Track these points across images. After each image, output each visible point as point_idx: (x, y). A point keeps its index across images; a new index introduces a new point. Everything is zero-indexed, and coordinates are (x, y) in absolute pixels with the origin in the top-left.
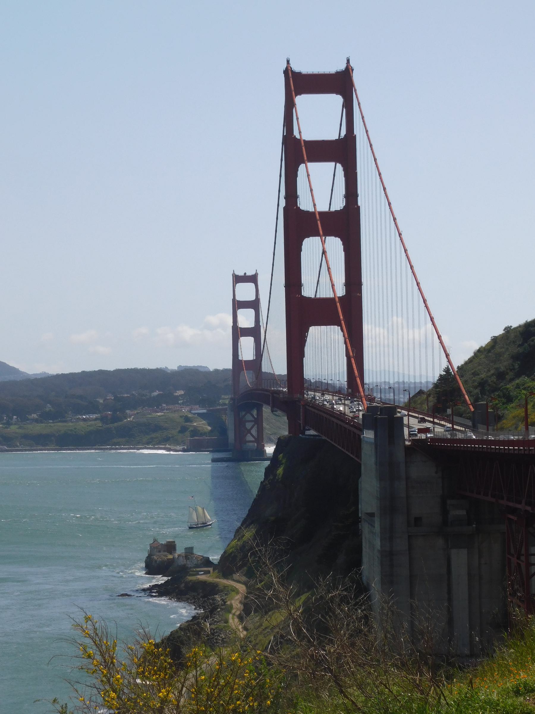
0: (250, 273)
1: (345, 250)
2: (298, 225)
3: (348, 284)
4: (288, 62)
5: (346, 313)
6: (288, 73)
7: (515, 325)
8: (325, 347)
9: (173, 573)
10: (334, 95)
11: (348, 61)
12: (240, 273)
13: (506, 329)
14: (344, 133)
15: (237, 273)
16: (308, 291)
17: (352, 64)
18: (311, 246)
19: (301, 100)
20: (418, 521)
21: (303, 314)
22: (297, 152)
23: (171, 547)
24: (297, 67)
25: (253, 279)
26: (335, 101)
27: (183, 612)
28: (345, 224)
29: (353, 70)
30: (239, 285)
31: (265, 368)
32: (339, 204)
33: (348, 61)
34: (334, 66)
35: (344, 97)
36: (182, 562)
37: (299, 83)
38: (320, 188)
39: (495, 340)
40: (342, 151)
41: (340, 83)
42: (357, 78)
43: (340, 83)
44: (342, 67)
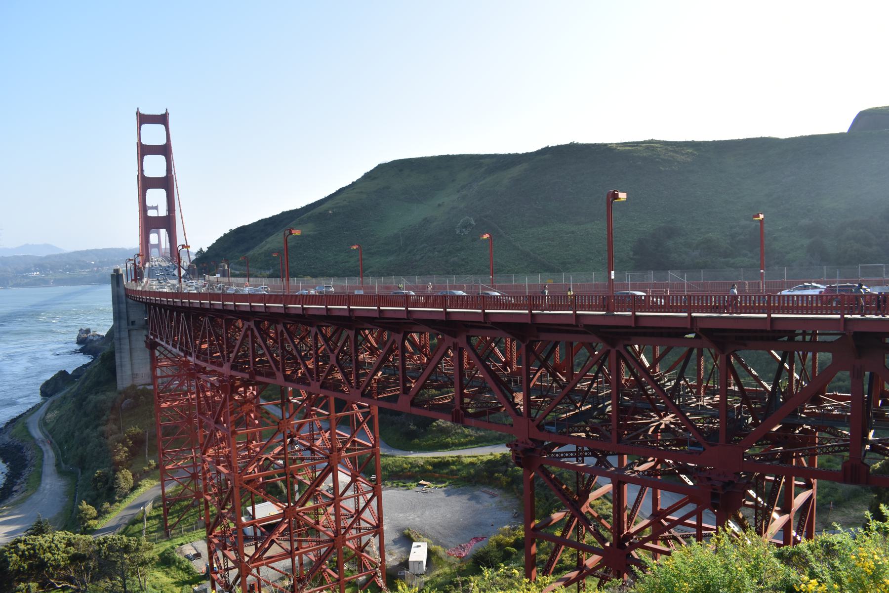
2: (146, 183)
5: (168, 223)
6: (138, 114)
7: (234, 228)
8: (158, 238)
9: (86, 343)
16: (151, 213)
19: (144, 126)
20: (133, 323)
22: (144, 150)
23: (88, 331)
24: (142, 112)
25: (156, 208)
28: (166, 183)
31: (163, 246)
34: (160, 112)
36: (91, 338)
37: (143, 119)
38: (155, 166)
39: (225, 235)
40: (165, 150)
43: (162, 119)
44: (164, 112)
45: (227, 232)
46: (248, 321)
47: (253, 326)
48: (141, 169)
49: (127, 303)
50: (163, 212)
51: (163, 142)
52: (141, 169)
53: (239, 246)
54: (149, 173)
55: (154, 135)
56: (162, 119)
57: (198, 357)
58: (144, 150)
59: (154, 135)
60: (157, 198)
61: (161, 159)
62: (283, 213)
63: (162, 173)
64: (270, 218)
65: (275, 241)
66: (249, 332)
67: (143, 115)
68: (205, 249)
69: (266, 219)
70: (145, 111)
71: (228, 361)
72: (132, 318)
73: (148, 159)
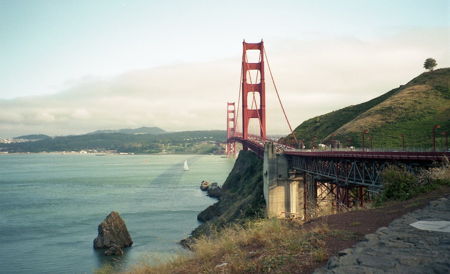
0: (233, 102)
2: (246, 88)
3: (261, 106)
5: (260, 114)
8: (254, 124)
12: (230, 102)
17: (263, 41)
18: (250, 95)
19: (248, 52)
20: (280, 176)
21: (247, 114)
22: (246, 67)
24: (246, 42)
25: (233, 104)
27: (212, 202)
28: (260, 88)
30: (229, 106)
31: (237, 130)
32: (259, 82)
37: (247, 46)
38: (253, 77)
40: (260, 66)
41: (260, 46)
42: (264, 45)
43: (260, 46)
44: (260, 42)
48: (244, 80)
49: (277, 163)
50: (259, 108)
52: (244, 80)
53: (314, 129)
55: (253, 56)
59: (253, 56)
65: (351, 127)
67: (248, 44)
72: (280, 173)
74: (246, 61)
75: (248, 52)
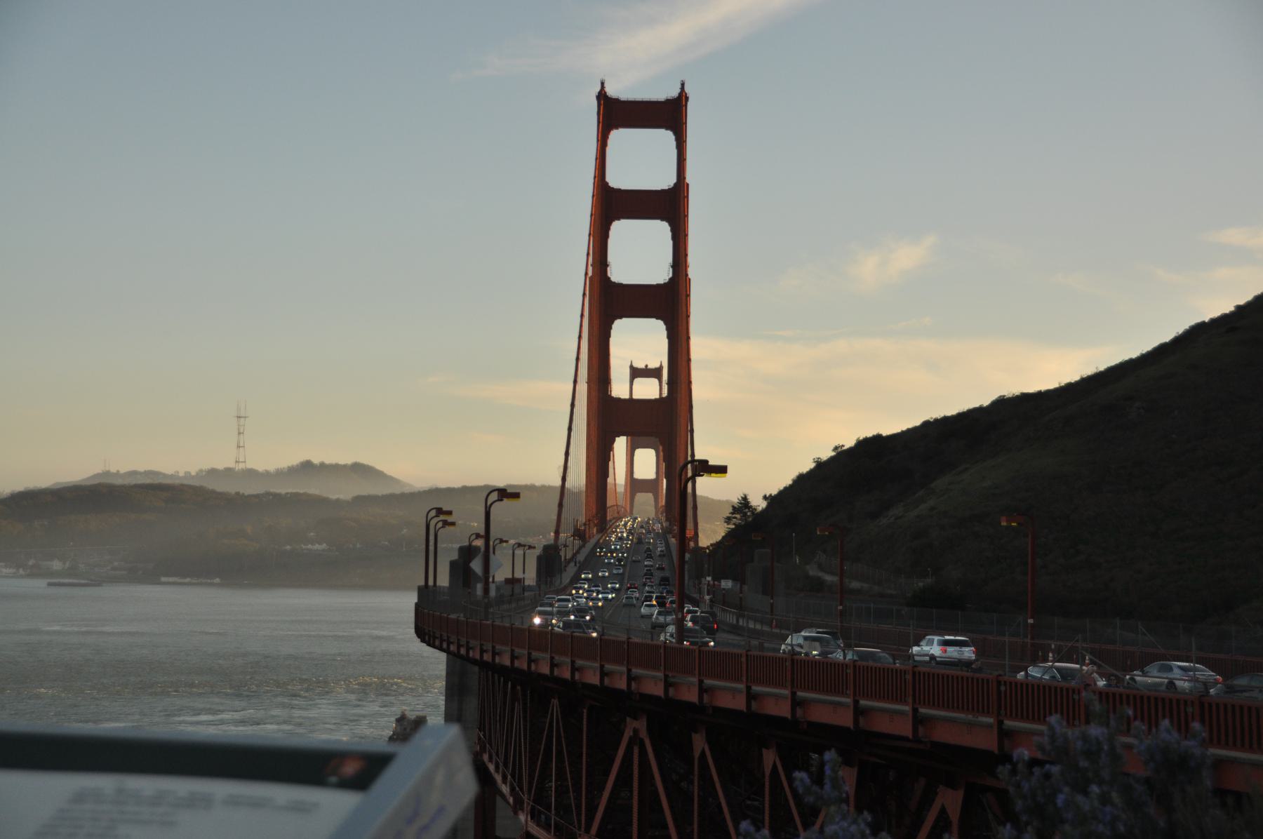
0: (653, 365)
1: (669, 337)
4: (602, 84)
5: (665, 422)
10: (662, 131)
11: (683, 85)
12: (640, 365)
13: (836, 448)
14: (674, 180)
15: (635, 365)
16: (619, 389)
17: (687, 89)
21: (610, 419)
24: (611, 91)
25: (655, 373)
26: (665, 138)
28: (667, 302)
29: (687, 99)
30: (637, 381)
33: (683, 85)
35: (675, 134)
37: (616, 113)
38: (640, 253)
40: (668, 206)
43: (668, 114)
44: (674, 93)
45: (826, 454)
46: (635, 719)
47: (644, 734)
51: (663, 180)
54: (620, 272)
55: (641, 160)
56: (668, 114)
57: (534, 815)
58: (613, 205)
59: (641, 160)
60: (638, 343)
61: (659, 230)
62: (1001, 404)
63: (657, 272)
64: (961, 416)
66: (636, 750)
67: (617, 101)
68: (759, 504)
69: (945, 419)
70: (619, 90)
71: (588, 830)
73: (623, 231)
74: (608, 179)
75: (620, 138)
